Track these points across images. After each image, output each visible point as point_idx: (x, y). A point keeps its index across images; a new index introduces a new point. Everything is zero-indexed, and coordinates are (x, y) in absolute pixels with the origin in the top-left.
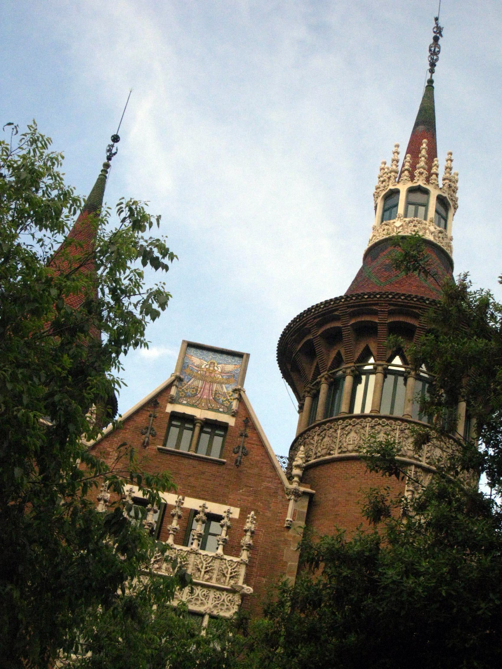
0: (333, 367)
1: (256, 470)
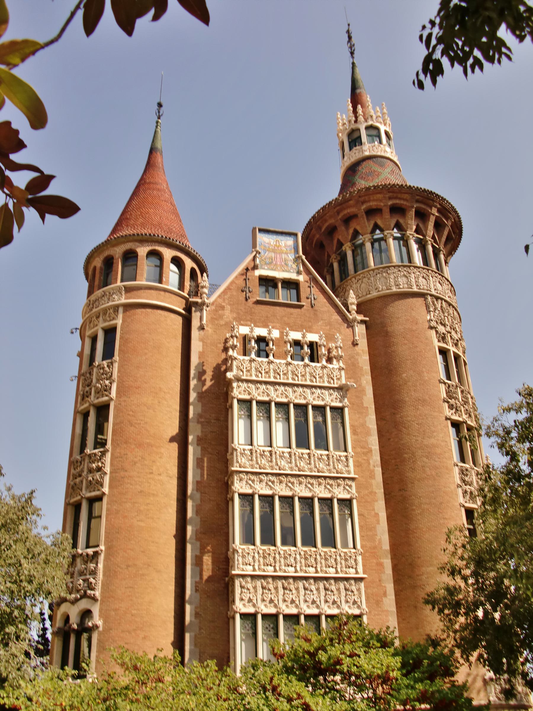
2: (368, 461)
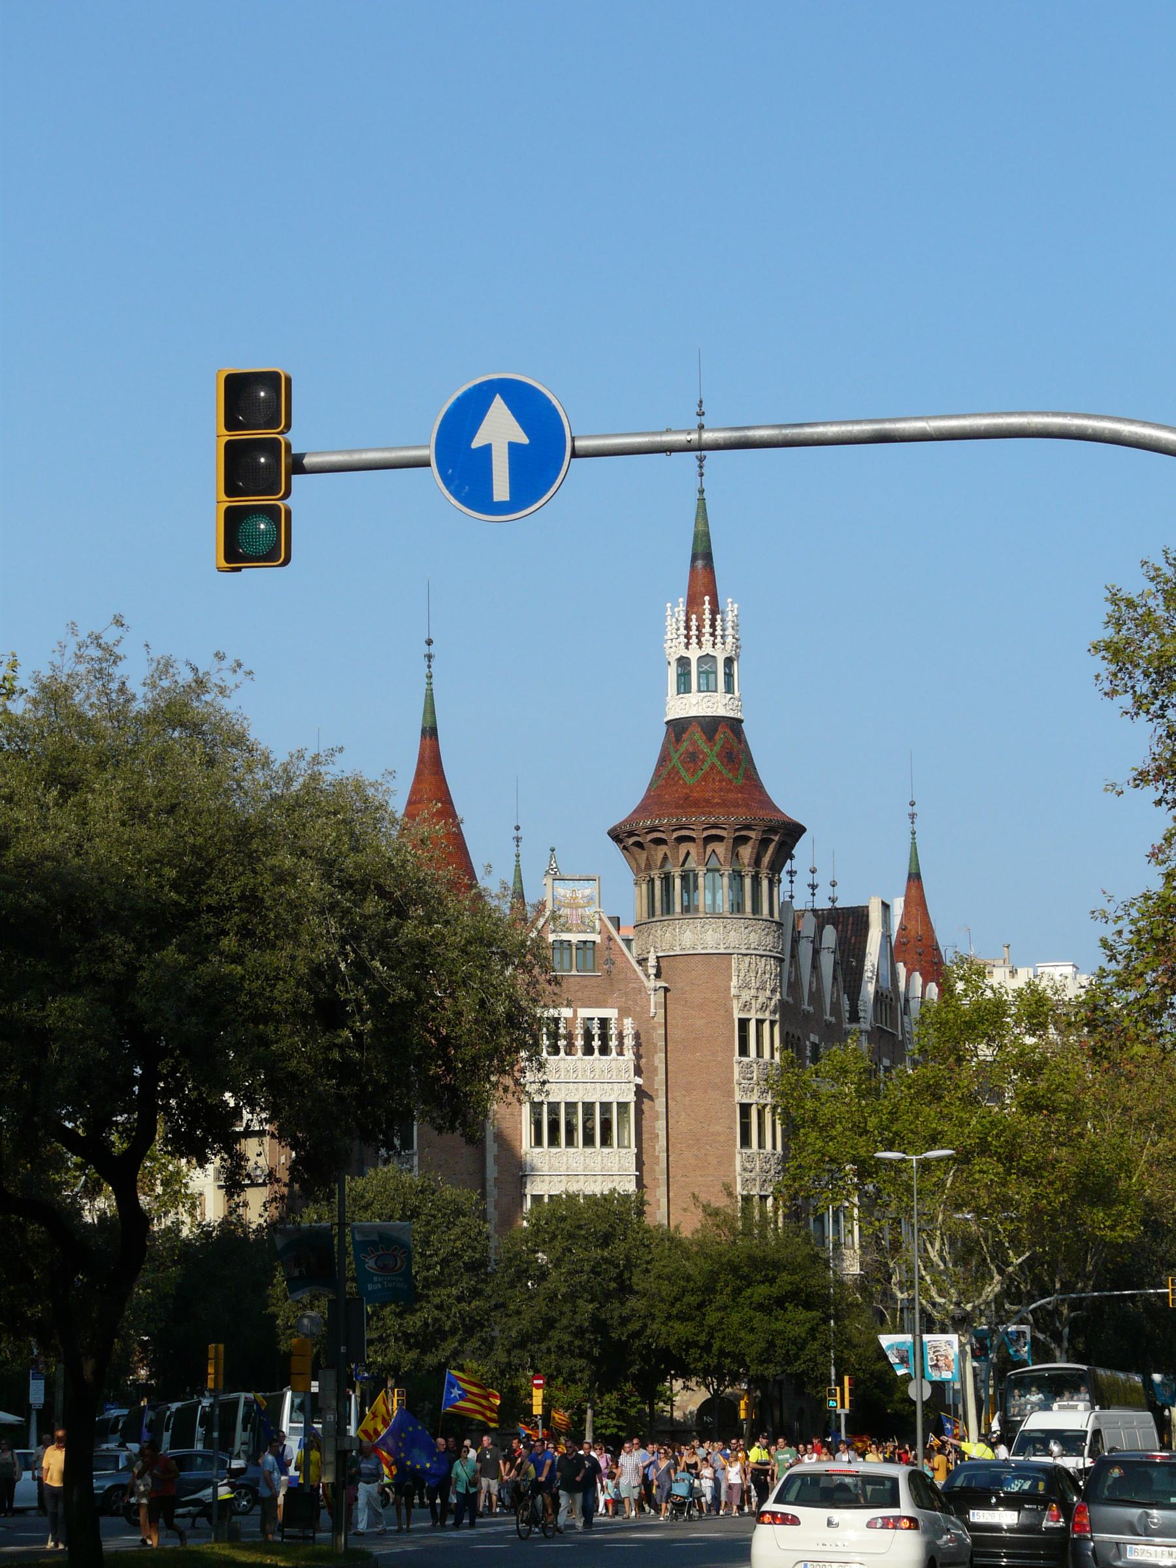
0: (662, 866)
1: (622, 976)
2: (654, 1147)
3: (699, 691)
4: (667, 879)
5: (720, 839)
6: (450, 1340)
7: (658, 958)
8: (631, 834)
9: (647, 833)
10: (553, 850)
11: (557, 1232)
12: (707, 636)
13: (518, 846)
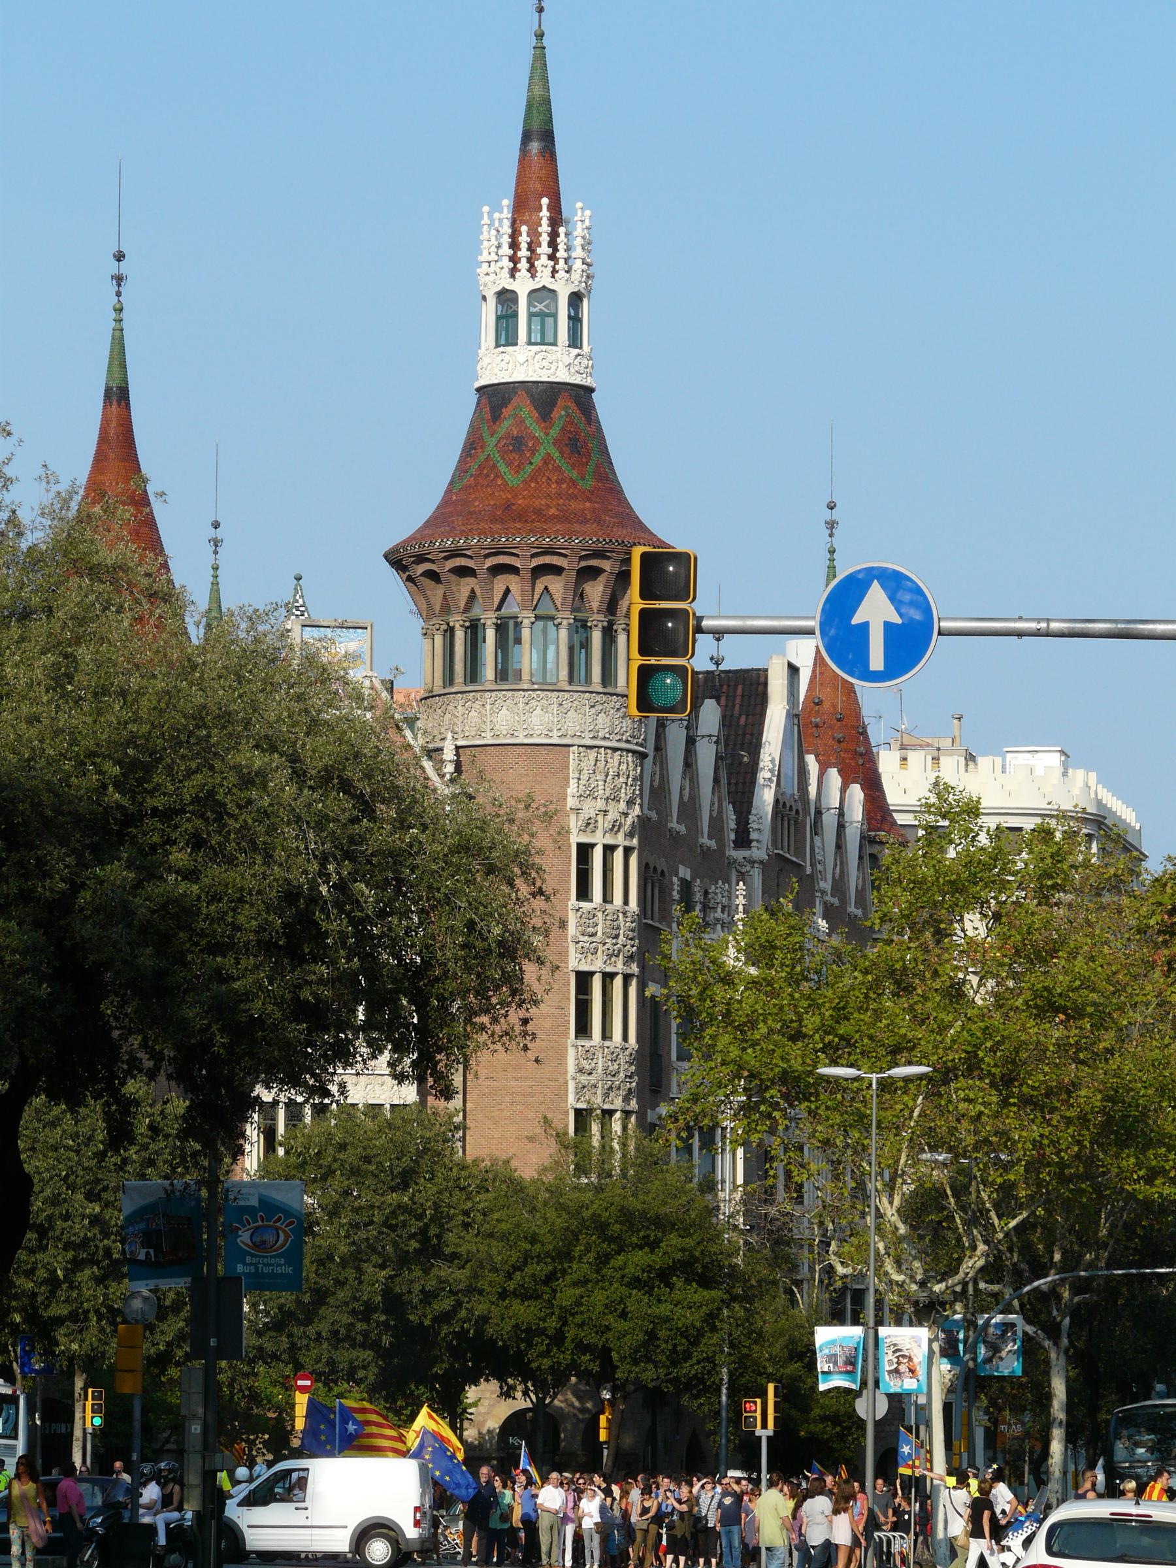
0: (467, 609)
3: (530, 343)
4: (474, 630)
5: (557, 570)
6: (171, 1319)
7: (457, 748)
8: (421, 559)
9: (446, 558)
10: (298, 578)
11: (335, 1166)
12: (544, 260)
13: (216, 553)
